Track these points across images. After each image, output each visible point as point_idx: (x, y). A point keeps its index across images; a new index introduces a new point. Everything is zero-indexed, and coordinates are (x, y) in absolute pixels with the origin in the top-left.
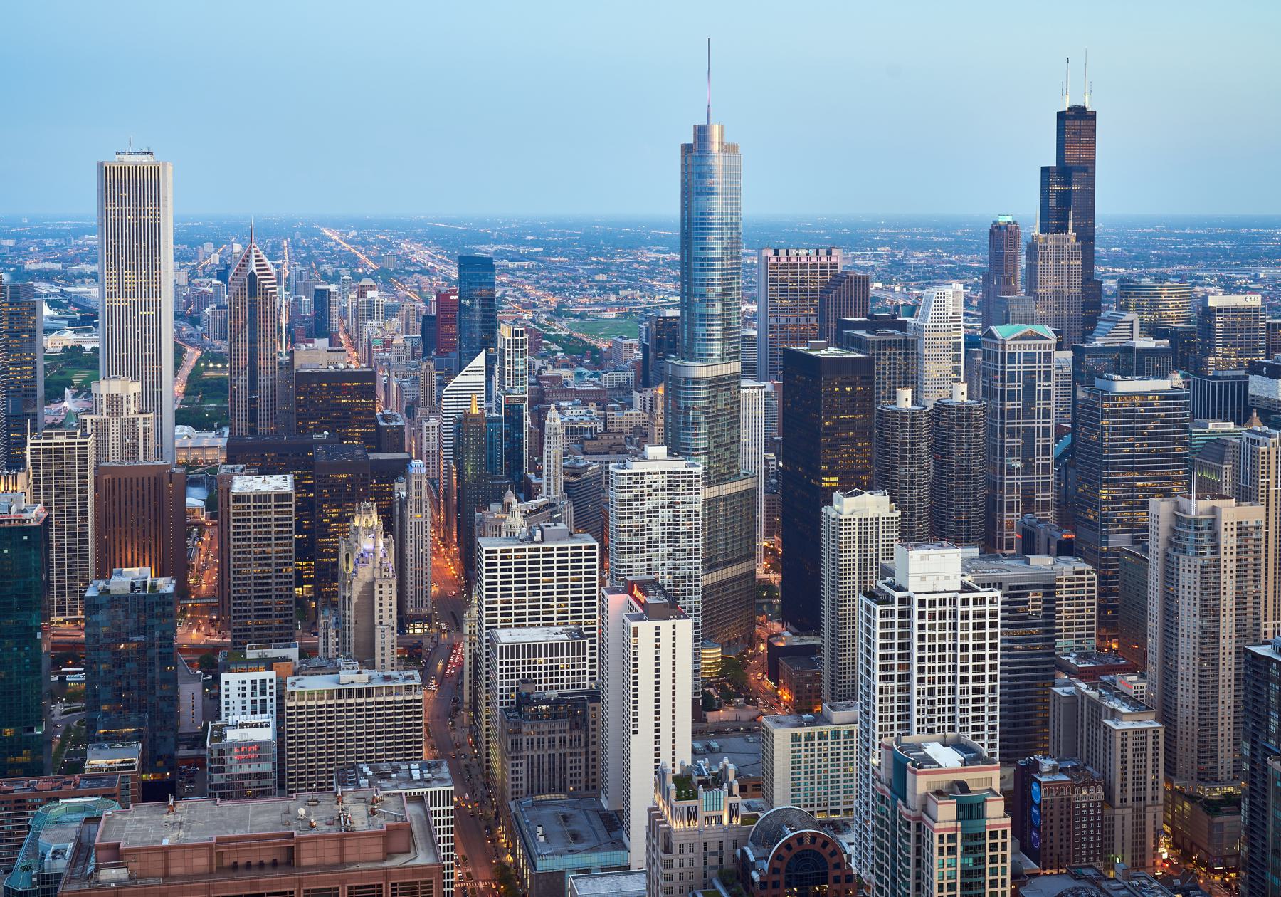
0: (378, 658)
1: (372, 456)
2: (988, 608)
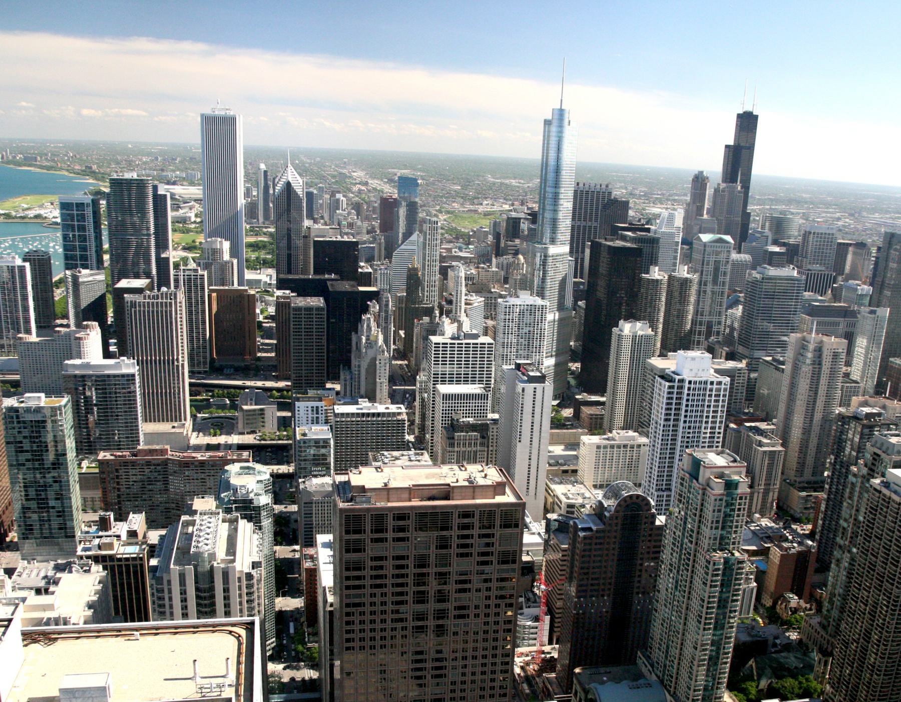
0: (378, 397)
1: (361, 289)
2: (723, 386)
